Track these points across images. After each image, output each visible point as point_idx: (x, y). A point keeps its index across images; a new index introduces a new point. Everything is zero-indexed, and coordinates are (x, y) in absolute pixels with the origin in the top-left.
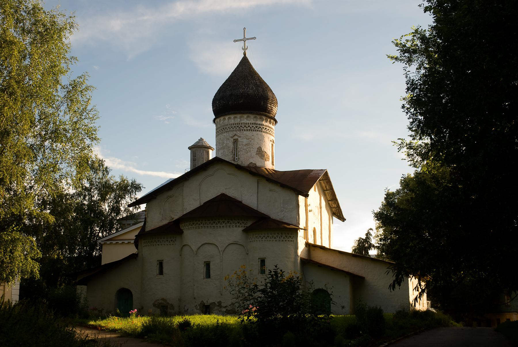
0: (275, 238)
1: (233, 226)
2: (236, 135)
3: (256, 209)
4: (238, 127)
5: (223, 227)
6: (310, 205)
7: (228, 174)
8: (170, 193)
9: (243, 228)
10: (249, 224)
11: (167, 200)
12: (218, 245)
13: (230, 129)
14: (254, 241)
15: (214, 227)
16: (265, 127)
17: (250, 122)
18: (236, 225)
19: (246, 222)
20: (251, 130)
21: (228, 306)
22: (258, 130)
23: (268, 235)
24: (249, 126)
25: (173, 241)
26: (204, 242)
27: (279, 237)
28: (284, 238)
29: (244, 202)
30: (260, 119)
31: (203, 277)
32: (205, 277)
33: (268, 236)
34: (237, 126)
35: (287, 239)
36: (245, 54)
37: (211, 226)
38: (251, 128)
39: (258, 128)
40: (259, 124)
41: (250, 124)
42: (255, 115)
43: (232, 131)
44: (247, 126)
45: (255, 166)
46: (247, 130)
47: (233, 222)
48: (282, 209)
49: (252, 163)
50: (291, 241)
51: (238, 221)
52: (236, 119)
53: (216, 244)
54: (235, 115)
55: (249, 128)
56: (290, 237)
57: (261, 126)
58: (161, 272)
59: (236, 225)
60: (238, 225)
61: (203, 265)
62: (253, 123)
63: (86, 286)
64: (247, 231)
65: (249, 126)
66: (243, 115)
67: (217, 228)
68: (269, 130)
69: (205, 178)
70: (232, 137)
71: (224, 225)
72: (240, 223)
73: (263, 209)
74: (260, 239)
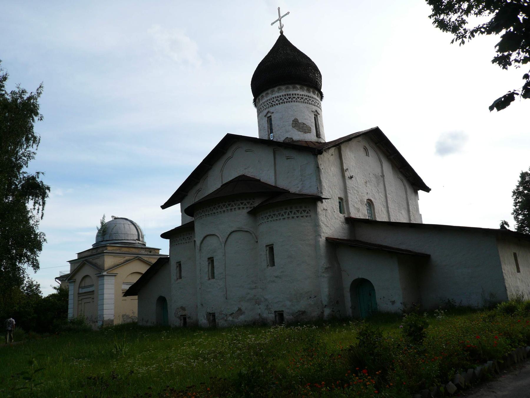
0: (283, 215)
1: (235, 209)
2: (269, 113)
3: (274, 185)
4: (270, 103)
5: (224, 211)
6: (347, 169)
7: (246, 151)
8: (198, 187)
9: (249, 210)
10: (257, 203)
11: (197, 195)
12: (219, 236)
13: (264, 107)
14: (261, 224)
15: (215, 213)
16: (302, 97)
17: (281, 94)
18: (239, 207)
19: (253, 202)
20: (284, 102)
21: (234, 313)
22: (291, 101)
23: (274, 213)
24: (281, 99)
25: (189, 238)
26: (205, 235)
27: (287, 214)
28: (295, 214)
29: (262, 180)
30: (293, 89)
31: (208, 277)
32: (210, 277)
33: (274, 215)
34: (269, 102)
35: (299, 214)
36: (282, 32)
37: (211, 214)
38: (283, 100)
39: (292, 99)
40: (293, 94)
41: (281, 96)
42: (286, 86)
43: (265, 109)
44: (279, 99)
45: (291, 140)
46: (280, 104)
47: (234, 204)
48: (300, 177)
49: (287, 138)
50: (307, 216)
51: (242, 202)
52: (268, 95)
53: (217, 234)
54: (266, 92)
55: (281, 101)
56: (304, 211)
57: (295, 96)
58: (180, 277)
59: (239, 207)
60: (241, 206)
61: (207, 263)
62: (285, 95)
63: (137, 296)
64: (254, 213)
65: (281, 99)
66: (274, 89)
67: (218, 215)
68: (308, 99)
69: (226, 161)
70: (265, 116)
71: (224, 209)
72: (244, 204)
73: (283, 184)
74: (266, 220)
